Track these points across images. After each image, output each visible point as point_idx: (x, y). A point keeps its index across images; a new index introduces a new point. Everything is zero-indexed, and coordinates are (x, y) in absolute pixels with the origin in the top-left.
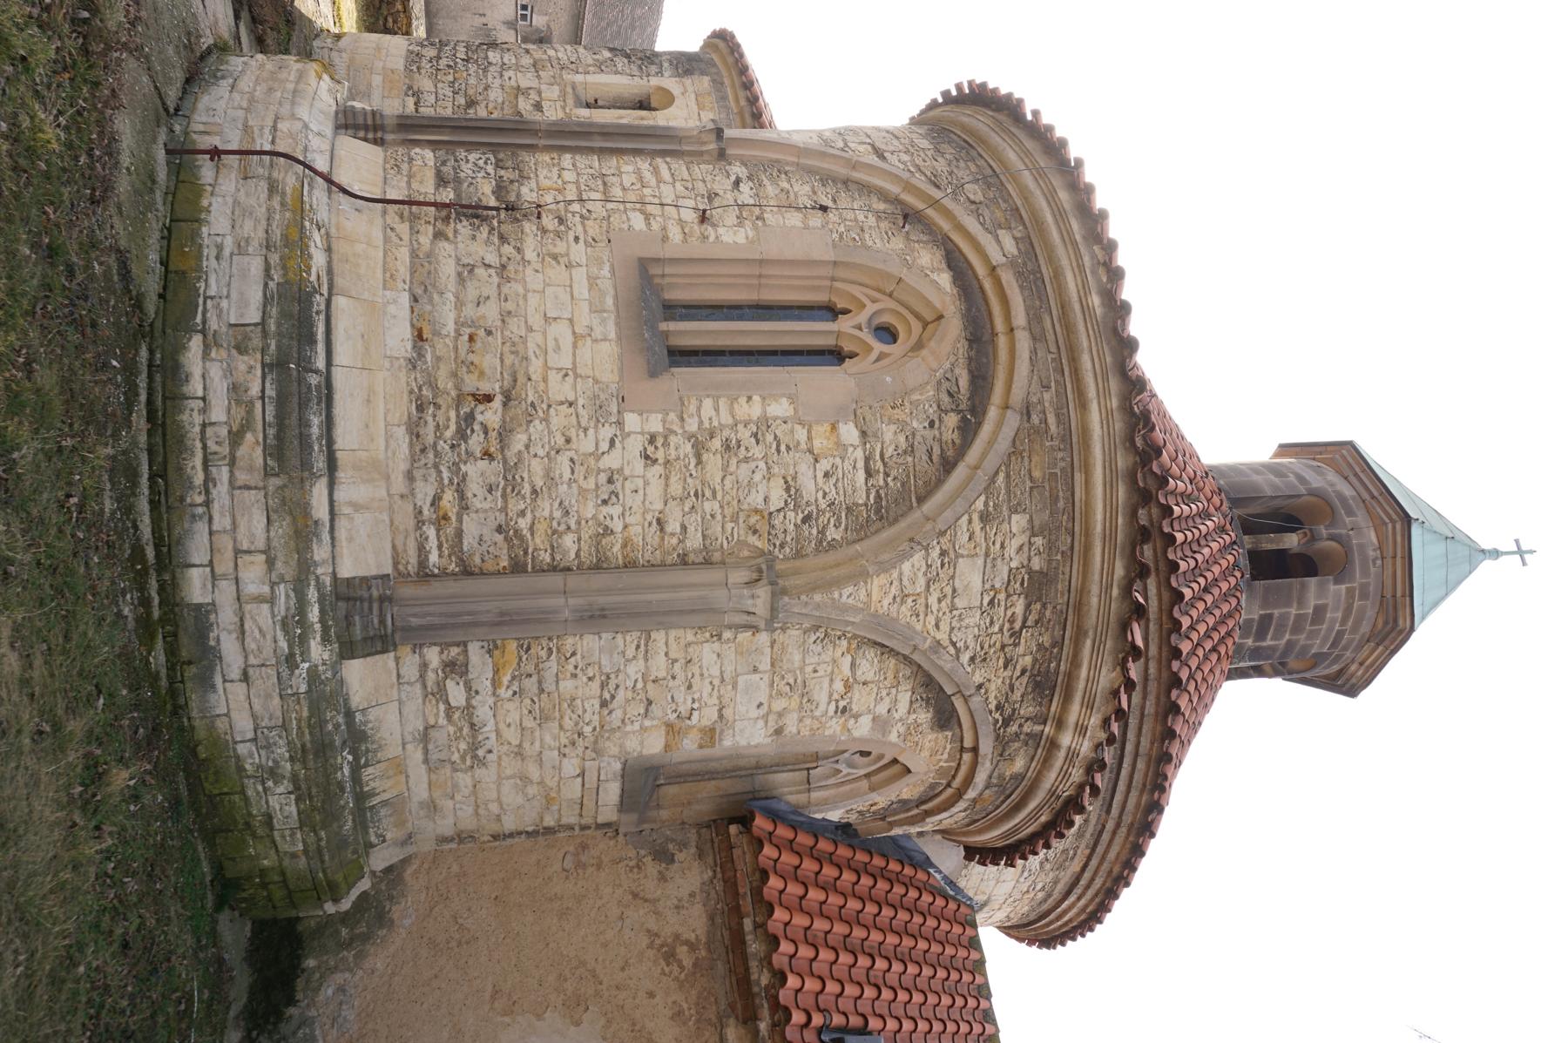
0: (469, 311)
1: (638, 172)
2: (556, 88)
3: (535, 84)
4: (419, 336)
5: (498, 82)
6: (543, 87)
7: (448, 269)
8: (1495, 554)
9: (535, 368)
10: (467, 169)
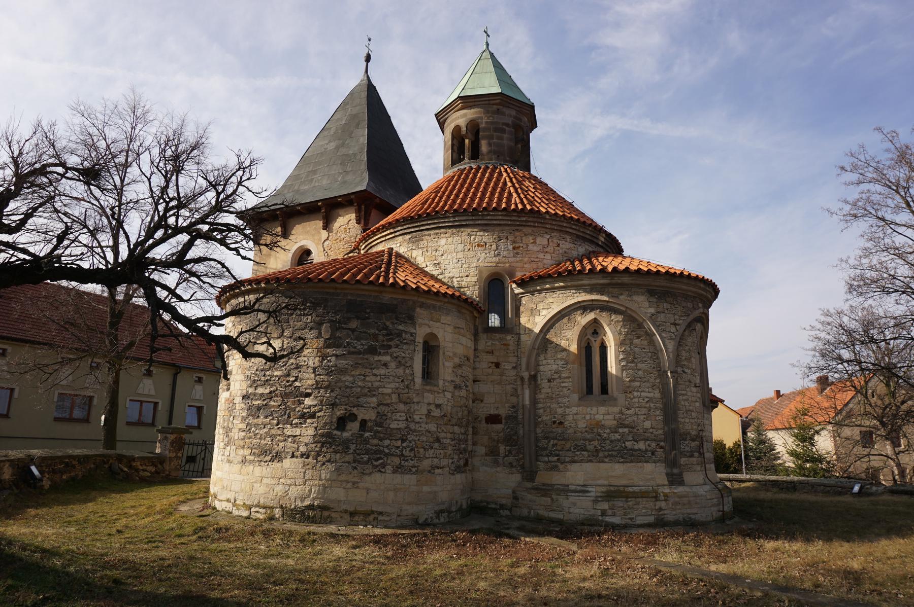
2: (425, 394)
5: (423, 425)
6: (426, 401)
8: (487, 44)
10: (687, 449)
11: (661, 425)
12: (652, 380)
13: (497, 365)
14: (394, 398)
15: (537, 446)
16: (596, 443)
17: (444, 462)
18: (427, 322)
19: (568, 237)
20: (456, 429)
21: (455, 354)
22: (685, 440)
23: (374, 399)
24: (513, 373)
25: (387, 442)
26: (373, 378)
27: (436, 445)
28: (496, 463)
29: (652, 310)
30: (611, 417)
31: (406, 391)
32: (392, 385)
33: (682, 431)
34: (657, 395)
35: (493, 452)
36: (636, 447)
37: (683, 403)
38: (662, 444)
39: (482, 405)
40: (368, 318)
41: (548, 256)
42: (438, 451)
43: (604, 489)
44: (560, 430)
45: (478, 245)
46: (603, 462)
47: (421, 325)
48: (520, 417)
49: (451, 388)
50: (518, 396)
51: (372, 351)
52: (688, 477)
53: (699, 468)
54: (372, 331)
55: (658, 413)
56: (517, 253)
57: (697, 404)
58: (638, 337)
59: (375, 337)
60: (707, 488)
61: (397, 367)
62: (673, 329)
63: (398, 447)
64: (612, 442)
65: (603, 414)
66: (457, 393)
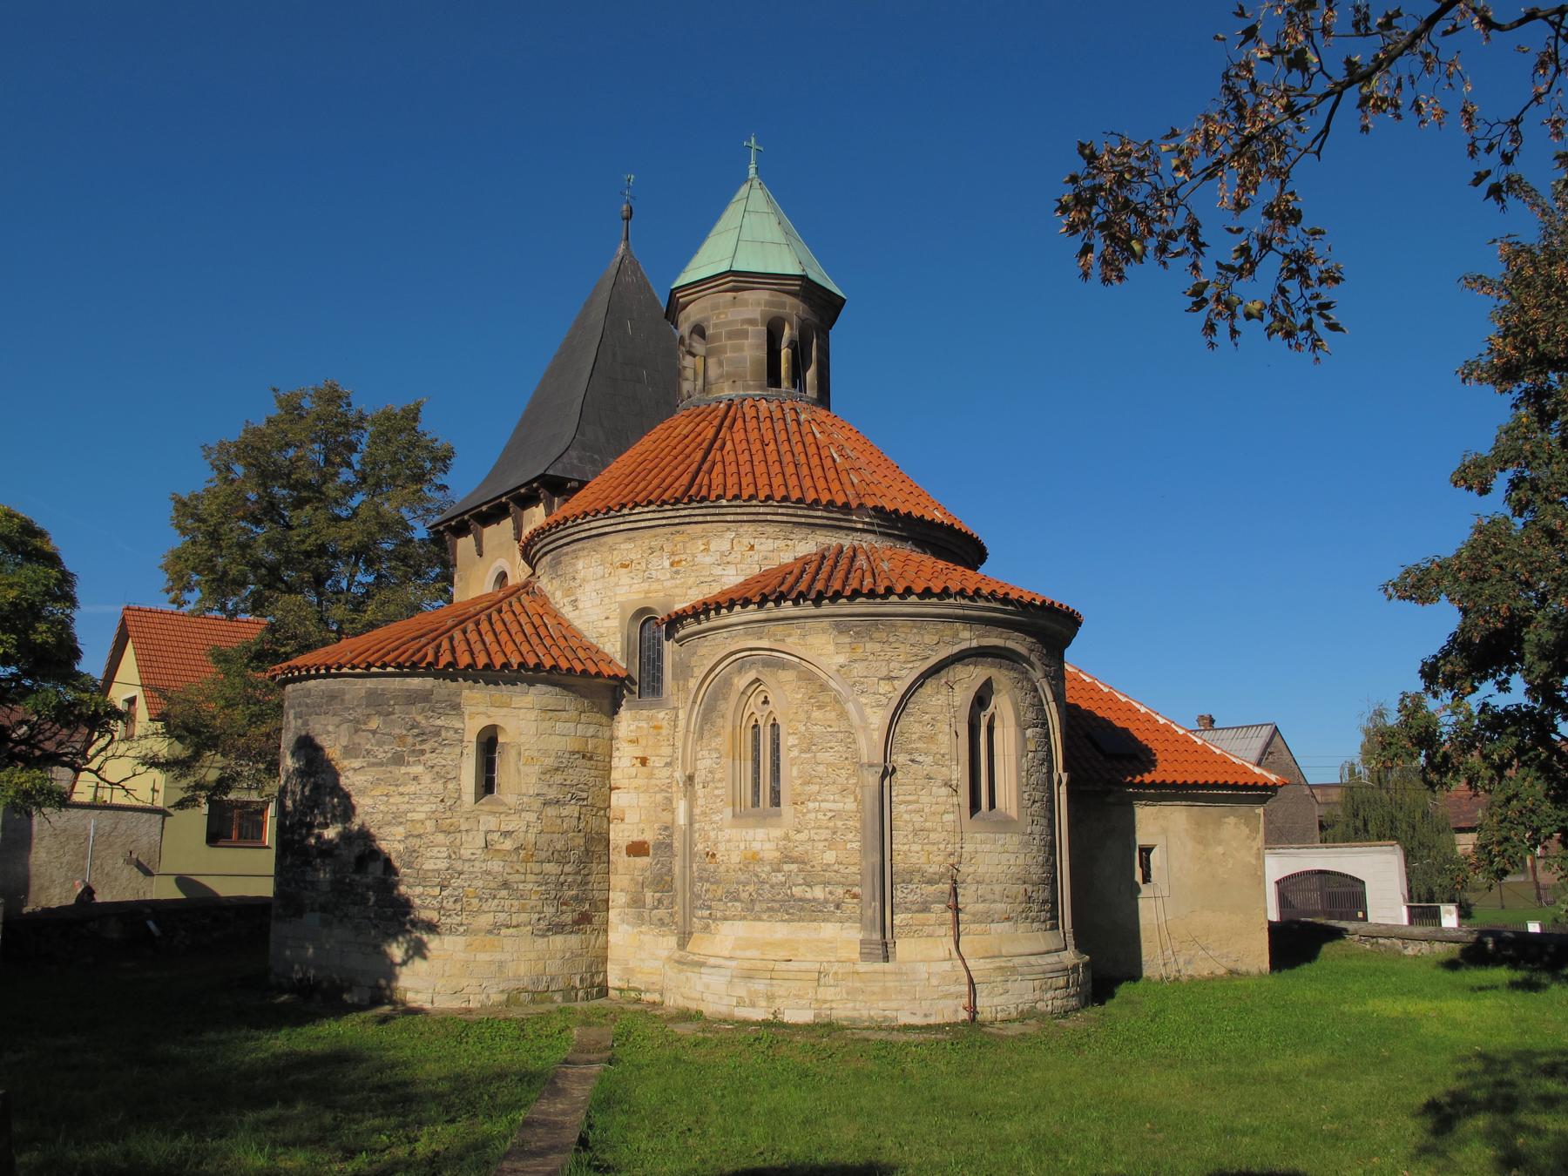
0: (997, 897)
1: (910, 812)
3: (482, 835)
4: (1008, 919)
5: (477, 864)
7: (981, 907)
9: (1013, 869)
11: (856, 858)
12: (840, 780)
13: (644, 761)
14: (430, 825)
15: (693, 893)
16: (751, 888)
17: (523, 917)
18: (482, 709)
19: (769, 529)
20: (551, 868)
21: (546, 753)
22: (910, 882)
23: (401, 829)
24: (666, 772)
25: (419, 890)
26: (398, 799)
27: (504, 893)
28: (641, 920)
29: (841, 659)
30: (772, 846)
31: (449, 814)
32: (427, 808)
33: (901, 866)
34: (850, 805)
35: (636, 902)
36: (808, 895)
37: (906, 817)
38: (856, 890)
39: (622, 826)
40: (392, 713)
41: (731, 570)
42: (507, 903)
43: (747, 965)
44: (711, 867)
45: (624, 566)
46: (760, 919)
47: (472, 716)
48: (676, 844)
49: (537, 805)
50: (673, 811)
51: (398, 760)
52: (904, 948)
53: (942, 931)
54: (397, 731)
55: (850, 836)
56: (677, 572)
57: (949, 817)
58: (820, 707)
59: (402, 738)
60: (947, 966)
61: (434, 780)
62: (884, 687)
63: (435, 897)
64: (772, 887)
65: (763, 840)
66: (551, 811)
